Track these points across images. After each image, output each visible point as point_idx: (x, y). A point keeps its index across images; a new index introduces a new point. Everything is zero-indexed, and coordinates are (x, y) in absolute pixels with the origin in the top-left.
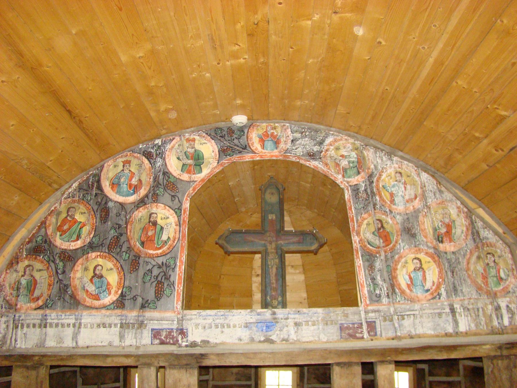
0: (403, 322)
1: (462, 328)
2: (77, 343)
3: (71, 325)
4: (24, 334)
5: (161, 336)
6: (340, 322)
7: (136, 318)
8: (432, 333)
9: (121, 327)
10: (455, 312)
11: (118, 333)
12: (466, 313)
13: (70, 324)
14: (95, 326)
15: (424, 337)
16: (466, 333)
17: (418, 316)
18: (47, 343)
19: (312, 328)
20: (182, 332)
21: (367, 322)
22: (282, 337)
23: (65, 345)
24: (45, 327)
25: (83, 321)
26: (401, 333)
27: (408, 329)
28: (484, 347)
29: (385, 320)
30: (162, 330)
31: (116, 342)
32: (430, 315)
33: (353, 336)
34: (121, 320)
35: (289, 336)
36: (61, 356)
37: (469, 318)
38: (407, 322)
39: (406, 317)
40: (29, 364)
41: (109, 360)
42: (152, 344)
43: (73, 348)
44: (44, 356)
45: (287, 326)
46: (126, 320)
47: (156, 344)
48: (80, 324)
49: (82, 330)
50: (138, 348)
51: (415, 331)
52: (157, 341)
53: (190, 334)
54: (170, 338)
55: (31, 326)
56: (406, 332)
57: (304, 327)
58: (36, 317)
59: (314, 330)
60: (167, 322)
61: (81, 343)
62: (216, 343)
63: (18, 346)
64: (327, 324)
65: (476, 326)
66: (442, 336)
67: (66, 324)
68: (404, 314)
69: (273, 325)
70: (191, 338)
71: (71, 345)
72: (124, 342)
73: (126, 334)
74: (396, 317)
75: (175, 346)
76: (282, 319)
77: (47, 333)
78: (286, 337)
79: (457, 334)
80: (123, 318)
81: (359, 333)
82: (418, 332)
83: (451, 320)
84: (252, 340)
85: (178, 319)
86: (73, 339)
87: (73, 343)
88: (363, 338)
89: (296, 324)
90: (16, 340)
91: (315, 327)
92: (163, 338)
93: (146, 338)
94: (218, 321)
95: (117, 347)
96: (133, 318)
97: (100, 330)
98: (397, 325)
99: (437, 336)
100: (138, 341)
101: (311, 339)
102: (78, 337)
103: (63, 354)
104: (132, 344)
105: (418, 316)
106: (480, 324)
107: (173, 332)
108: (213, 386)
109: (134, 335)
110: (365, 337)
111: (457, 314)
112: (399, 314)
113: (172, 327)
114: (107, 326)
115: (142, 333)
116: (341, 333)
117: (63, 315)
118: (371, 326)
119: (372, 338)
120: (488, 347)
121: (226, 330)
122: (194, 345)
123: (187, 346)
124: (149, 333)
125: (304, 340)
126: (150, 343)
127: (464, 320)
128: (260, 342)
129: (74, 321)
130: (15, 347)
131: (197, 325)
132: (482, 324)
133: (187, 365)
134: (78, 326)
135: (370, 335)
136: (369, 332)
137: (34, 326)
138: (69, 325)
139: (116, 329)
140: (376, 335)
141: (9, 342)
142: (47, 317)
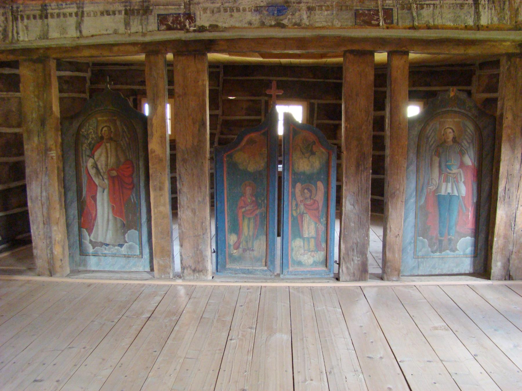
0: (422, 11)
1: (484, 21)
2: (81, 32)
3: (74, 14)
4: (26, 26)
6: (355, 8)
7: (141, 4)
8: (452, 24)
9: (126, 14)
10: (479, 4)
11: (123, 21)
12: (490, 6)
13: (72, 13)
14: (99, 14)
15: (443, 29)
16: (487, 27)
17: (438, 6)
19: (326, 13)
20: (190, 17)
21: (383, 9)
22: (294, 21)
23: (69, 36)
24: (46, 17)
25: (85, 9)
26: (418, 23)
27: (426, 19)
28: (504, 43)
29: (403, 9)
30: (169, 15)
31: (122, 29)
32: (451, 5)
33: (368, 23)
34: (125, 6)
35: (301, 20)
36: (66, 47)
37: (493, 11)
38: (426, 12)
39: (425, 6)
40: (35, 57)
42: (158, 29)
43: (78, 38)
44: (48, 49)
45: (299, 11)
46: (130, 6)
47: (163, 30)
48: (83, 12)
49: (86, 19)
50: (144, 35)
51: (434, 21)
53: (198, 19)
54: (177, 23)
55: (32, 17)
56: (423, 22)
57: (318, 12)
58: (35, 8)
59: (328, 15)
60: (173, 7)
61: (85, 32)
62: (225, 28)
64: (341, 10)
65: (499, 20)
66: (461, 29)
67: (68, 14)
68: (423, 3)
69: (285, 9)
70: (200, 22)
71: (75, 36)
72: (130, 29)
73: (131, 20)
74: (415, 6)
75: (183, 32)
76: (294, 3)
78: (298, 22)
79: (478, 28)
80: (127, 4)
81: (375, 20)
82: (436, 23)
83: (472, 12)
84: (263, 24)
85: (185, 3)
86: (76, 29)
87: (77, 32)
88: (378, 25)
89: (310, 9)
91: (329, 12)
92: (170, 23)
93: (153, 23)
94: (227, 5)
95: (122, 34)
96: (137, 3)
97: (103, 18)
98: (415, 14)
99: (457, 28)
100: (144, 27)
101: (325, 24)
102: (82, 27)
103: (67, 46)
104: (138, 31)
105: (438, 6)
106: (504, 18)
107: (180, 17)
108: (223, 120)
109: (139, 21)
110: (381, 24)
111: (480, 6)
112: (418, 2)
113: (180, 12)
114: (111, 13)
115: (148, 19)
116: (355, 19)
117: (64, 4)
118: (388, 13)
119: (388, 25)
120: (508, 43)
121: (235, 14)
122: (202, 29)
123: (194, 31)
125: (317, 25)
126: (157, 29)
127: (487, 13)
128: (271, 26)
129: (75, 10)
130: (18, 40)
131: (205, 10)
132: (506, 18)
133: (195, 51)
134: (80, 15)
135: (386, 23)
136: (385, 20)
137: (35, 17)
138: (71, 15)
139: (120, 16)
140: (392, 22)
142: (48, 7)
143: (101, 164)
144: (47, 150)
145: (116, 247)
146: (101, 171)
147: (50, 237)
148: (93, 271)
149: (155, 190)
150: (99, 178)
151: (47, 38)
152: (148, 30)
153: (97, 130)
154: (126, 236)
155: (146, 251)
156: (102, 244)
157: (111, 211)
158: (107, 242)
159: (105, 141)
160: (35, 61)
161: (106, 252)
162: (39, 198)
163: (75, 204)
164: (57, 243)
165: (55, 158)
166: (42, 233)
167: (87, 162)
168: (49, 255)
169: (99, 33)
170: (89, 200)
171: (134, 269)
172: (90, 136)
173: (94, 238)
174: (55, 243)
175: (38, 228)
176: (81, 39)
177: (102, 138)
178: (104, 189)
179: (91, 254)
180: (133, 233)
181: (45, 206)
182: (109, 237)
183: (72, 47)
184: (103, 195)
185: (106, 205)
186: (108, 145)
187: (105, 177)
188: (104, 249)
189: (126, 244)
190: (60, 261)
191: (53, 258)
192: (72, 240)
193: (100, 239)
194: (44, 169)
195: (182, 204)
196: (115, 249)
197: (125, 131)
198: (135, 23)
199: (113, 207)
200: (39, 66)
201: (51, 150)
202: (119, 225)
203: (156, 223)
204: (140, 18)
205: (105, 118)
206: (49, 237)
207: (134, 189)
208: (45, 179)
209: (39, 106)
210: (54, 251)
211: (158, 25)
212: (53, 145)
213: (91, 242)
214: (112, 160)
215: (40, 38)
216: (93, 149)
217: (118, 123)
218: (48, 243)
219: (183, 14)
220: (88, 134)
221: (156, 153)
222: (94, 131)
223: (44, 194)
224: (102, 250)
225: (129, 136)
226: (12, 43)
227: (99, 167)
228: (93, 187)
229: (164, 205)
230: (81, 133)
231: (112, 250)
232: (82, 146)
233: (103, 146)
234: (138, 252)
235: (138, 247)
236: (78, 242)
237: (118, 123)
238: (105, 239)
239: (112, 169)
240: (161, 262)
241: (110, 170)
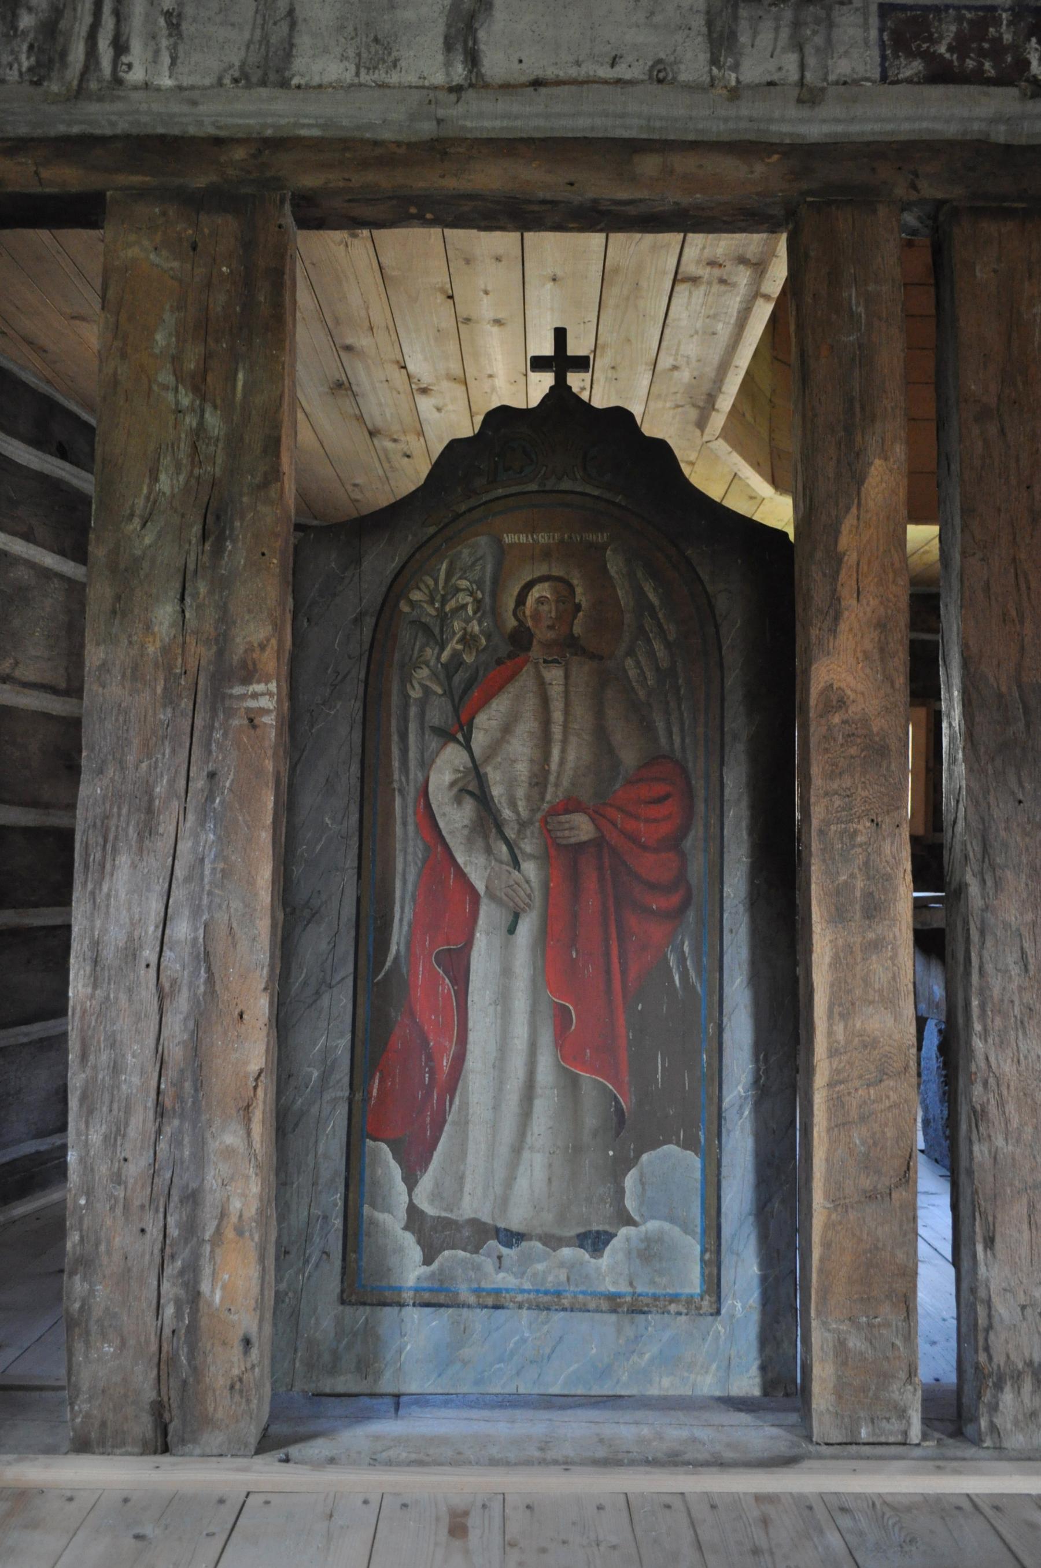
2: (473, 59)
4: (168, 14)
5: (930, 39)
18: (299, 64)
30: (937, 9)
31: (694, 63)
36: (376, 143)
40: (200, 181)
41: (649, 165)
42: (884, 78)
43: (456, 90)
47: (909, 81)
52: (915, 67)
54: (982, 53)
61: (496, 63)
63: (136, 76)
72: (736, 67)
73: (744, 25)
75: (1013, 92)
77: (299, 13)
86: (449, 47)
87: (448, 64)
90: (120, 47)
92: (942, 49)
95: (690, 88)
100: (811, 61)
102: (481, 34)
103: (387, 135)
104: (775, 77)
107: (997, 23)
109: (785, 33)
115: (831, 25)
124: (866, 26)
126: (877, 75)
141: (77, 54)
143: (510, 778)
144: (230, 671)
145: (567, 1252)
146: (507, 813)
147: (193, 1198)
148: (422, 1400)
149: (839, 916)
150: (489, 851)
151: (284, 84)
152: (832, 78)
153: (495, 595)
154: (630, 1181)
155: (743, 1271)
156: (481, 1234)
157: (546, 1038)
158: (516, 1219)
159: (536, 652)
160: (195, 202)
161: (503, 1279)
162: (149, 954)
163: (341, 1000)
164: (230, 1234)
165: (269, 720)
166: (136, 1168)
167: (426, 765)
168: (169, 1311)
169: (573, 72)
170: (423, 976)
171: (664, 1385)
172: (457, 625)
173: (436, 1196)
174: (218, 1232)
175: (116, 1136)
176: (470, 94)
177: (520, 640)
178: (516, 917)
179: (408, 1296)
180: (674, 1163)
181: (182, 1004)
182: (530, 1191)
183: (410, 145)
184: (507, 947)
185: (521, 1004)
186: (554, 675)
187: (528, 846)
188: (489, 1265)
189: (624, 1231)
190: (238, 1348)
191: (193, 1329)
192: (299, 1217)
193: (473, 1205)
194: (199, 783)
195: (996, 992)
196: (553, 1266)
197: (651, 608)
198: (765, 37)
199: (561, 1018)
200: (224, 228)
201: (248, 673)
202: (590, 1121)
203: (837, 1104)
204: (788, 15)
205: (542, 538)
206: (179, 1198)
207: (691, 915)
208: (197, 842)
209: (199, 432)
210: (205, 1287)
211: (884, 58)
212: (262, 647)
213: (415, 1217)
214: (571, 756)
215: (243, 79)
216: (466, 694)
217: (615, 565)
218: (173, 1232)
219: (1011, 9)
220: (443, 618)
221: (854, 710)
222: (478, 602)
223: (181, 929)
224: (478, 1268)
225: (672, 631)
226: (79, 93)
227: (497, 791)
228: (452, 901)
229: (888, 1001)
230: (405, 608)
231: (540, 1267)
232: (406, 680)
233: (526, 679)
234: (693, 1282)
235: (692, 1248)
236: (338, 1223)
237: (615, 565)
238: (504, 1203)
239: (571, 805)
240: (855, 1343)
241: (556, 811)
